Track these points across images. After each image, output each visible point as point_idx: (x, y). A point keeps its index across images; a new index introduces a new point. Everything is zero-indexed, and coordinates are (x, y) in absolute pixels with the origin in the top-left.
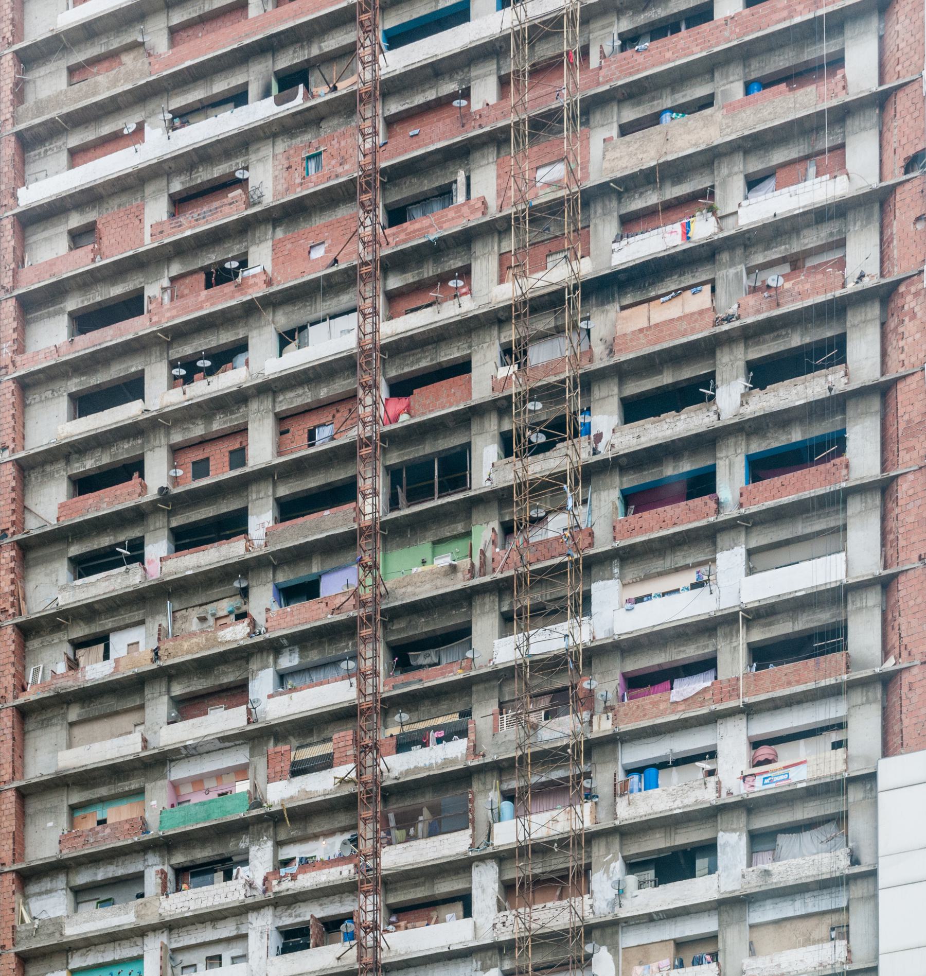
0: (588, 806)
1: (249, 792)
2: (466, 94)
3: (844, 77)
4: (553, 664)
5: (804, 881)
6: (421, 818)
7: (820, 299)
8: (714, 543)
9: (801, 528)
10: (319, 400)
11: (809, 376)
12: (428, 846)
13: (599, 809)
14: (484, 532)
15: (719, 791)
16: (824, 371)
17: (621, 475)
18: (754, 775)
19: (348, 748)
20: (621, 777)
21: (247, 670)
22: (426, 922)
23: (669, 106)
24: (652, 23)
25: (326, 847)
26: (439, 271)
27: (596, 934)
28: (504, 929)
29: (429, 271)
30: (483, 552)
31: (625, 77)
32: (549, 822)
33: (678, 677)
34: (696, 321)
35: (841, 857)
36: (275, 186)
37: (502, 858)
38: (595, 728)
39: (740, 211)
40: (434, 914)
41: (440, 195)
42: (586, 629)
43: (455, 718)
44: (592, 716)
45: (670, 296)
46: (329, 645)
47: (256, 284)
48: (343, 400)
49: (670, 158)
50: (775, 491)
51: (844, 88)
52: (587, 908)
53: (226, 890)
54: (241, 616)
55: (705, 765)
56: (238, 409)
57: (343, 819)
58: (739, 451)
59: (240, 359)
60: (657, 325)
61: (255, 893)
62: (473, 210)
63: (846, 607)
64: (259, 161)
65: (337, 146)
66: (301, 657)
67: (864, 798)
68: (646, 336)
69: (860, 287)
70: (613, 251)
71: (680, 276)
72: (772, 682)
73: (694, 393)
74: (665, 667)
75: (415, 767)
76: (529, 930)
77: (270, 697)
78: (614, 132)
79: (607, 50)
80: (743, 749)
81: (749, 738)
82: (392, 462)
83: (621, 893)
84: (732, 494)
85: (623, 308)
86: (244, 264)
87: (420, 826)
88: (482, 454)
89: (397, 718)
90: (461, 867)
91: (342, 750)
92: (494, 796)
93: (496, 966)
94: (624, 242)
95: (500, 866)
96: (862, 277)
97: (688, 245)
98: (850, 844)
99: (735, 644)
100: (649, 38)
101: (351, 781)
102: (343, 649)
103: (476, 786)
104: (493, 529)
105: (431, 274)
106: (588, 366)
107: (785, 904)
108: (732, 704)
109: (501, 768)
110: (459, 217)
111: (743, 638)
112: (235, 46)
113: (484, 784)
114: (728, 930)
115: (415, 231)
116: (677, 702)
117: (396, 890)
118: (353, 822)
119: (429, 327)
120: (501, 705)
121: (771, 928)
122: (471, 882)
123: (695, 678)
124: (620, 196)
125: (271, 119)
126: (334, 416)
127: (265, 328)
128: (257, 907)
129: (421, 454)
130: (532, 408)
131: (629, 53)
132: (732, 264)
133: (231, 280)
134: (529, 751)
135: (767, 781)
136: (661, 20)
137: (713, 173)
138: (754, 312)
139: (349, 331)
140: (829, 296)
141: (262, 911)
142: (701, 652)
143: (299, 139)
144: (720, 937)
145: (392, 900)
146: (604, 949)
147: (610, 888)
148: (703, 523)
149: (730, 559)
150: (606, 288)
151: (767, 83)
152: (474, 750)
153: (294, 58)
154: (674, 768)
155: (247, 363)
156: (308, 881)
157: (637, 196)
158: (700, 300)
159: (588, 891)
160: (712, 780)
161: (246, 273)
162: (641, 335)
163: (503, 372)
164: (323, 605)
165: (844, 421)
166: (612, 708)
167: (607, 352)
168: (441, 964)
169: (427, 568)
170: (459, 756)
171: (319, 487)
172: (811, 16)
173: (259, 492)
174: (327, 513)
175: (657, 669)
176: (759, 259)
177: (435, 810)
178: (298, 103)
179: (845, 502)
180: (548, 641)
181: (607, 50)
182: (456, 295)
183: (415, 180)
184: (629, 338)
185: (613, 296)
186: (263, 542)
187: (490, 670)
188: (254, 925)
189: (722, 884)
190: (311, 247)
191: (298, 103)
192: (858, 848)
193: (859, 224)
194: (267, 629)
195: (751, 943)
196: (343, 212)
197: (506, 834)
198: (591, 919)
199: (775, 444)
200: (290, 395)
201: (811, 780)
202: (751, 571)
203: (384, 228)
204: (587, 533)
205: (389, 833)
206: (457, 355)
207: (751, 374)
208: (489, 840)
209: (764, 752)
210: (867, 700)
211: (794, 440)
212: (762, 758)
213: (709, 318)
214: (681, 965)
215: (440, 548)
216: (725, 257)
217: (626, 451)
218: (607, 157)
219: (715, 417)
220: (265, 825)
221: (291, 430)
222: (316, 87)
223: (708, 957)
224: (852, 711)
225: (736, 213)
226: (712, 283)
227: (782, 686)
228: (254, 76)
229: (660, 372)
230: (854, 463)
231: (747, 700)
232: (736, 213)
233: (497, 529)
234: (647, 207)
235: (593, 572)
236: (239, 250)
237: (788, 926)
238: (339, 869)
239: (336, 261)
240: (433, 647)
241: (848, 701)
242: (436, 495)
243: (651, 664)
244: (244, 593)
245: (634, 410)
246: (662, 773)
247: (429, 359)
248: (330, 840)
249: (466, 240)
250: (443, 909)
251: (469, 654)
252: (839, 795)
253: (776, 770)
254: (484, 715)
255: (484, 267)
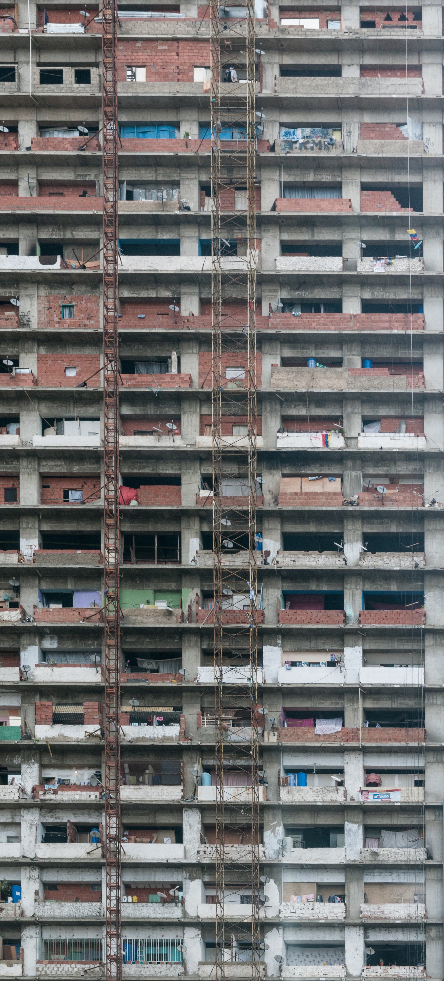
0: (261, 788)
1: (21, 727)
2: (178, 302)
3: (423, 377)
4: (240, 691)
5: (399, 863)
6: (147, 771)
7: (409, 508)
8: (343, 640)
9: (396, 645)
10: (72, 473)
11: (402, 554)
12: (153, 790)
13: (268, 791)
14: (191, 594)
15: (345, 796)
16: (411, 553)
17: (282, 581)
18: (368, 791)
19: (95, 714)
20: (282, 774)
21: (18, 642)
22: (149, 840)
23: (314, 356)
24: (303, 299)
25: (80, 776)
26: (158, 412)
27: (267, 870)
28: (205, 856)
29: (151, 410)
30: (190, 607)
31: (286, 329)
32: (235, 793)
33: (319, 718)
34: (332, 498)
35: (422, 853)
36: (39, 318)
37: (204, 809)
38: (266, 739)
39: (359, 438)
40: (155, 836)
41: (159, 362)
42: (259, 674)
43: (170, 710)
44: (263, 731)
45: (315, 478)
46: (80, 640)
47: (25, 381)
48: (90, 477)
49: (315, 390)
50: (381, 619)
51: (424, 383)
52: (261, 852)
53: (5, 790)
54: (14, 605)
55: (336, 778)
56: (12, 461)
57: (90, 760)
58: (358, 587)
59: (13, 427)
60: (306, 493)
61: (25, 797)
62: (183, 382)
63: (424, 700)
64: (27, 296)
65: (84, 305)
66: (59, 643)
67: (435, 820)
68: (299, 498)
69: (432, 508)
70: (278, 437)
71: (321, 466)
72: (379, 736)
73: (330, 543)
74: (310, 710)
75: (143, 737)
76: (223, 860)
77: (37, 666)
78: (278, 361)
79: (274, 307)
80: (361, 773)
81: (364, 767)
82: (125, 529)
83: (283, 848)
84: (354, 612)
85: (284, 476)
86: (16, 363)
87: (147, 776)
88: (189, 542)
89: (131, 702)
90: (176, 809)
91: (90, 714)
92: (197, 767)
93: (199, 878)
94: (285, 434)
95: (202, 813)
96: (433, 502)
97: (326, 450)
98: (427, 846)
99: (356, 707)
100: (299, 309)
101: (97, 736)
102: (90, 645)
103: (185, 758)
104: (197, 594)
105: (152, 413)
106: (261, 507)
107: (387, 874)
108: (354, 744)
109: (203, 751)
110: (173, 382)
111: (361, 704)
112: (10, 212)
113: (191, 758)
114: (351, 884)
115: (141, 382)
116: (319, 735)
117: (128, 814)
118: (98, 763)
119: (152, 449)
120: (202, 709)
121: (378, 887)
122: (182, 820)
123: (329, 721)
124: (282, 403)
125: (37, 271)
126: (83, 486)
127: (32, 412)
128: (28, 807)
129: (146, 530)
130: (224, 524)
131: (287, 314)
132: (354, 469)
133: (7, 372)
134: (223, 744)
135: (376, 797)
136: (308, 299)
137: (342, 407)
138: (367, 505)
139: (95, 434)
140: (414, 508)
141: (31, 810)
142: (333, 706)
143: (57, 291)
144: (346, 887)
145: (126, 821)
146: (272, 881)
147: (275, 842)
148: (336, 627)
149: (353, 654)
150: (274, 459)
151: (377, 363)
152: (184, 734)
153: (52, 234)
154: (316, 775)
155: (18, 432)
156: (65, 796)
157: (293, 406)
158: (334, 486)
159: (262, 842)
160: (341, 789)
161: (18, 371)
162: (296, 497)
163: (205, 493)
164: (77, 613)
165: (423, 586)
166: (277, 729)
167: (273, 500)
168: (161, 869)
169: (150, 607)
170: (174, 736)
171: (72, 532)
172: (403, 332)
173: (28, 523)
174: (79, 552)
175: (305, 710)
176: (371, 471)
177: (157, 768)
178: (56, 267)
179: (423, 636)
180: (238, 676)
181: (274, 307)
182: (170, 432)
183: (141, 347)
184: (288, 496)
185: (277, 466)
186: (31, 559)
187: (195, 685)
188: (25, 818)
189: (347, 854)
190: (66, 368)
191: (56, 267)
192: (431, 849)
193: (432, 469)
194: (34, 619)
195: (365, 894)
196: (88, 351)
197: (207, 794)
198: (263, 860)
199: (380, 589)
200: (51, 463)
201: (403, 802)
202: (365, 663)
203: (119, 373)
204: (261, 613)
205: (124, 777)
206: (171, 472)
207: (367, 543)
208: (194, 796)
209: (373, 777)
210: (437, 760)
211: (392, 590)
212: (372, 781)
213: (340, 499)
214: (321, 900)
215: (159, 595)
216: (349, 463)
217: (286, 568)
218: (274, 377)
219: (344, 562)
220: (33, 752)
221: (51, 486)
222: (68, 259)
223: (338, 898)
224: (428, 765)
225: (357, 438)
226: (341, 477)
227: (385, 740)
228: (24, 236)
229: (308, 523)
230: (429, 614)
231: (363, 744)
232: (357, 438)
233: (199, 594)
234: (300, 415)
235: (264, 639)
236: (12, 352)
237: (388, 888)
238: (89, 793)
239: (85, 384)
240: (155, 659)
241: (425, 759)
242: (156, 560)
243: (301, 706)
244: (17, 590)
245: (290, 543)
246: (309, 776)
247: (151, 469)
248: (81, 772)
249: (178, 398)
250: (161, 834)
251: (181, 672)
252: (420, 814)
253: (382, 791)
254: (191, 713)
255: (190, 421)
